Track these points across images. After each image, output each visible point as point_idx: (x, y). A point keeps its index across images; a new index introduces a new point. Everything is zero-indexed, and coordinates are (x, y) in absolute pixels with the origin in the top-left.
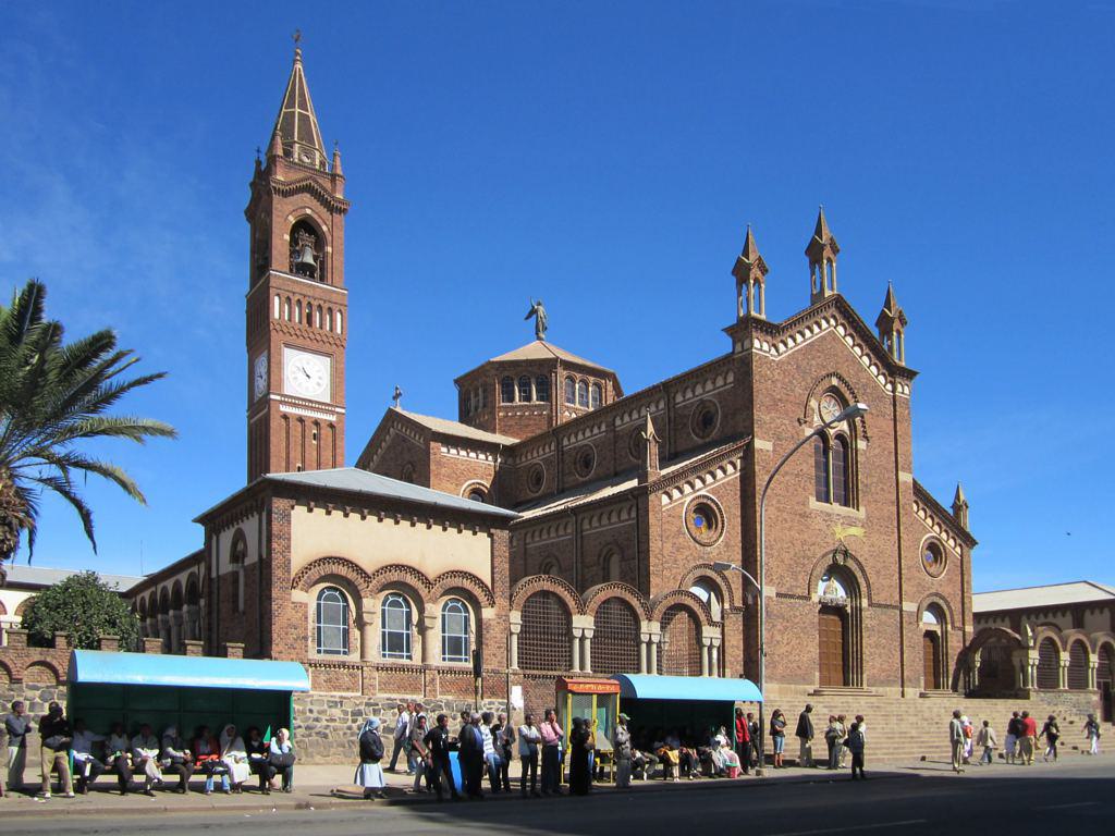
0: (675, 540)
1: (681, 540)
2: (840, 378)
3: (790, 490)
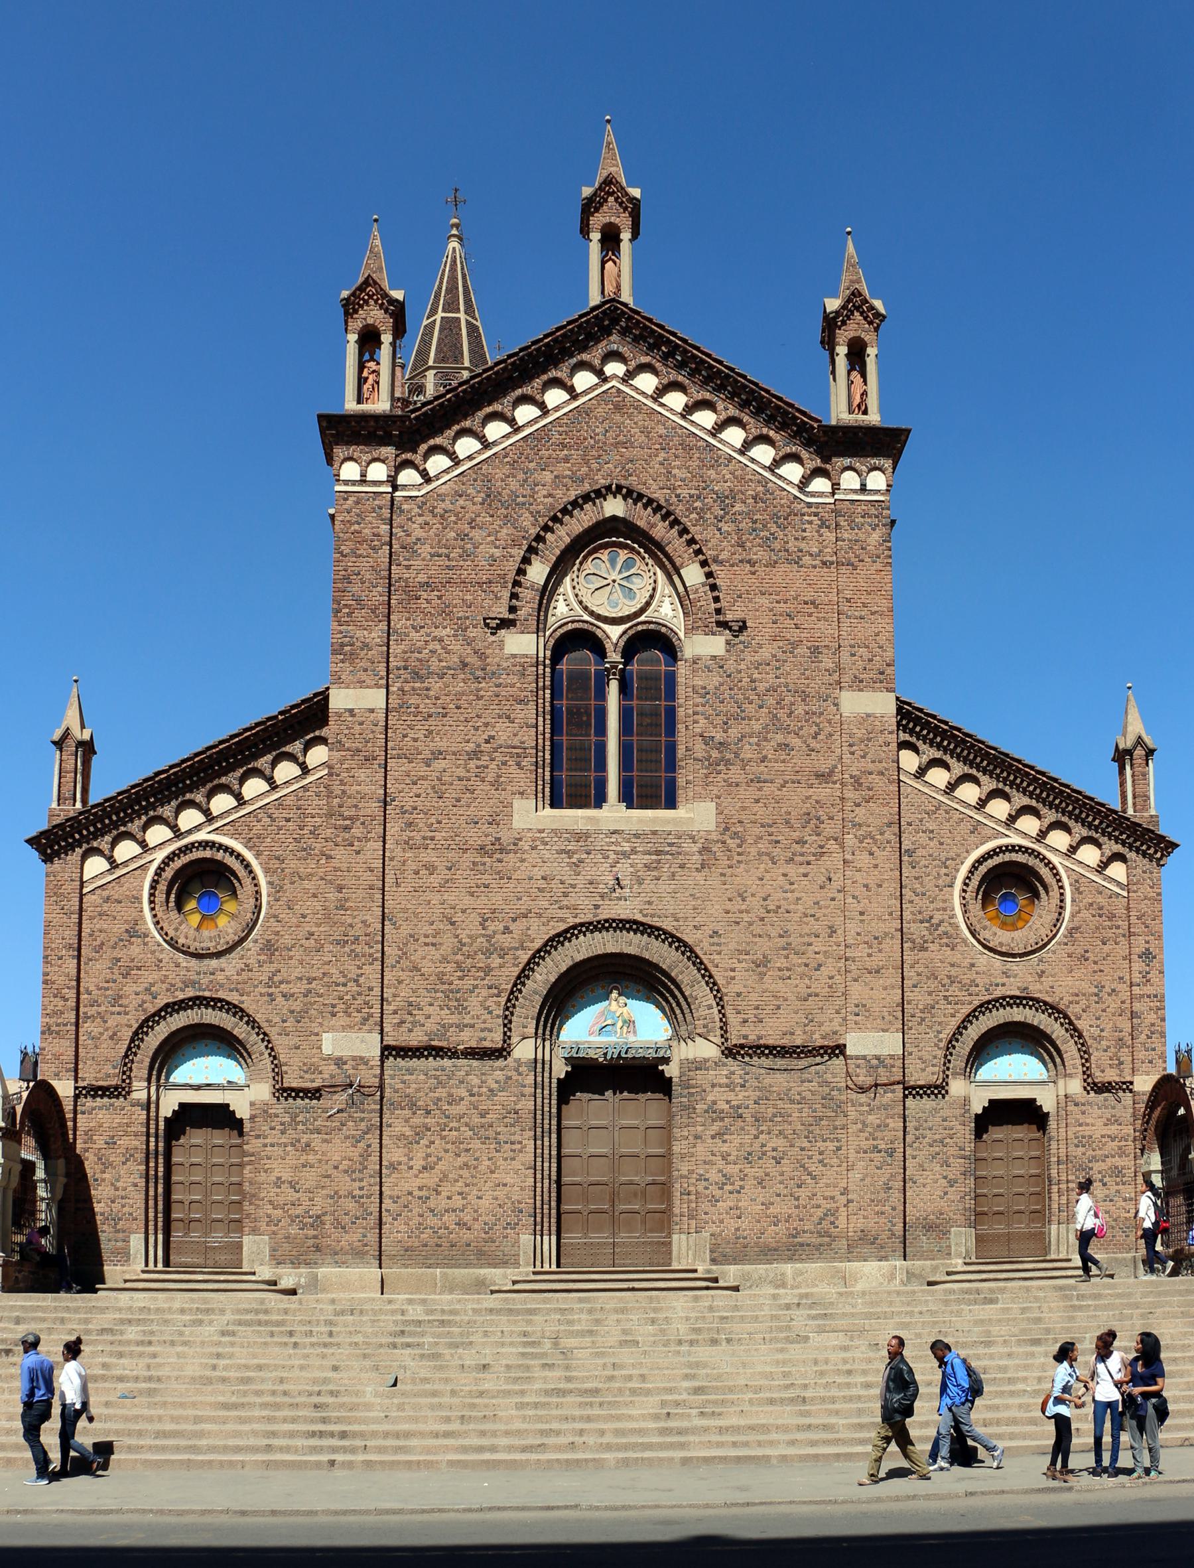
0: (117, 953)
1: (135, 950)
2: (630, 494)
3: (451, 794)
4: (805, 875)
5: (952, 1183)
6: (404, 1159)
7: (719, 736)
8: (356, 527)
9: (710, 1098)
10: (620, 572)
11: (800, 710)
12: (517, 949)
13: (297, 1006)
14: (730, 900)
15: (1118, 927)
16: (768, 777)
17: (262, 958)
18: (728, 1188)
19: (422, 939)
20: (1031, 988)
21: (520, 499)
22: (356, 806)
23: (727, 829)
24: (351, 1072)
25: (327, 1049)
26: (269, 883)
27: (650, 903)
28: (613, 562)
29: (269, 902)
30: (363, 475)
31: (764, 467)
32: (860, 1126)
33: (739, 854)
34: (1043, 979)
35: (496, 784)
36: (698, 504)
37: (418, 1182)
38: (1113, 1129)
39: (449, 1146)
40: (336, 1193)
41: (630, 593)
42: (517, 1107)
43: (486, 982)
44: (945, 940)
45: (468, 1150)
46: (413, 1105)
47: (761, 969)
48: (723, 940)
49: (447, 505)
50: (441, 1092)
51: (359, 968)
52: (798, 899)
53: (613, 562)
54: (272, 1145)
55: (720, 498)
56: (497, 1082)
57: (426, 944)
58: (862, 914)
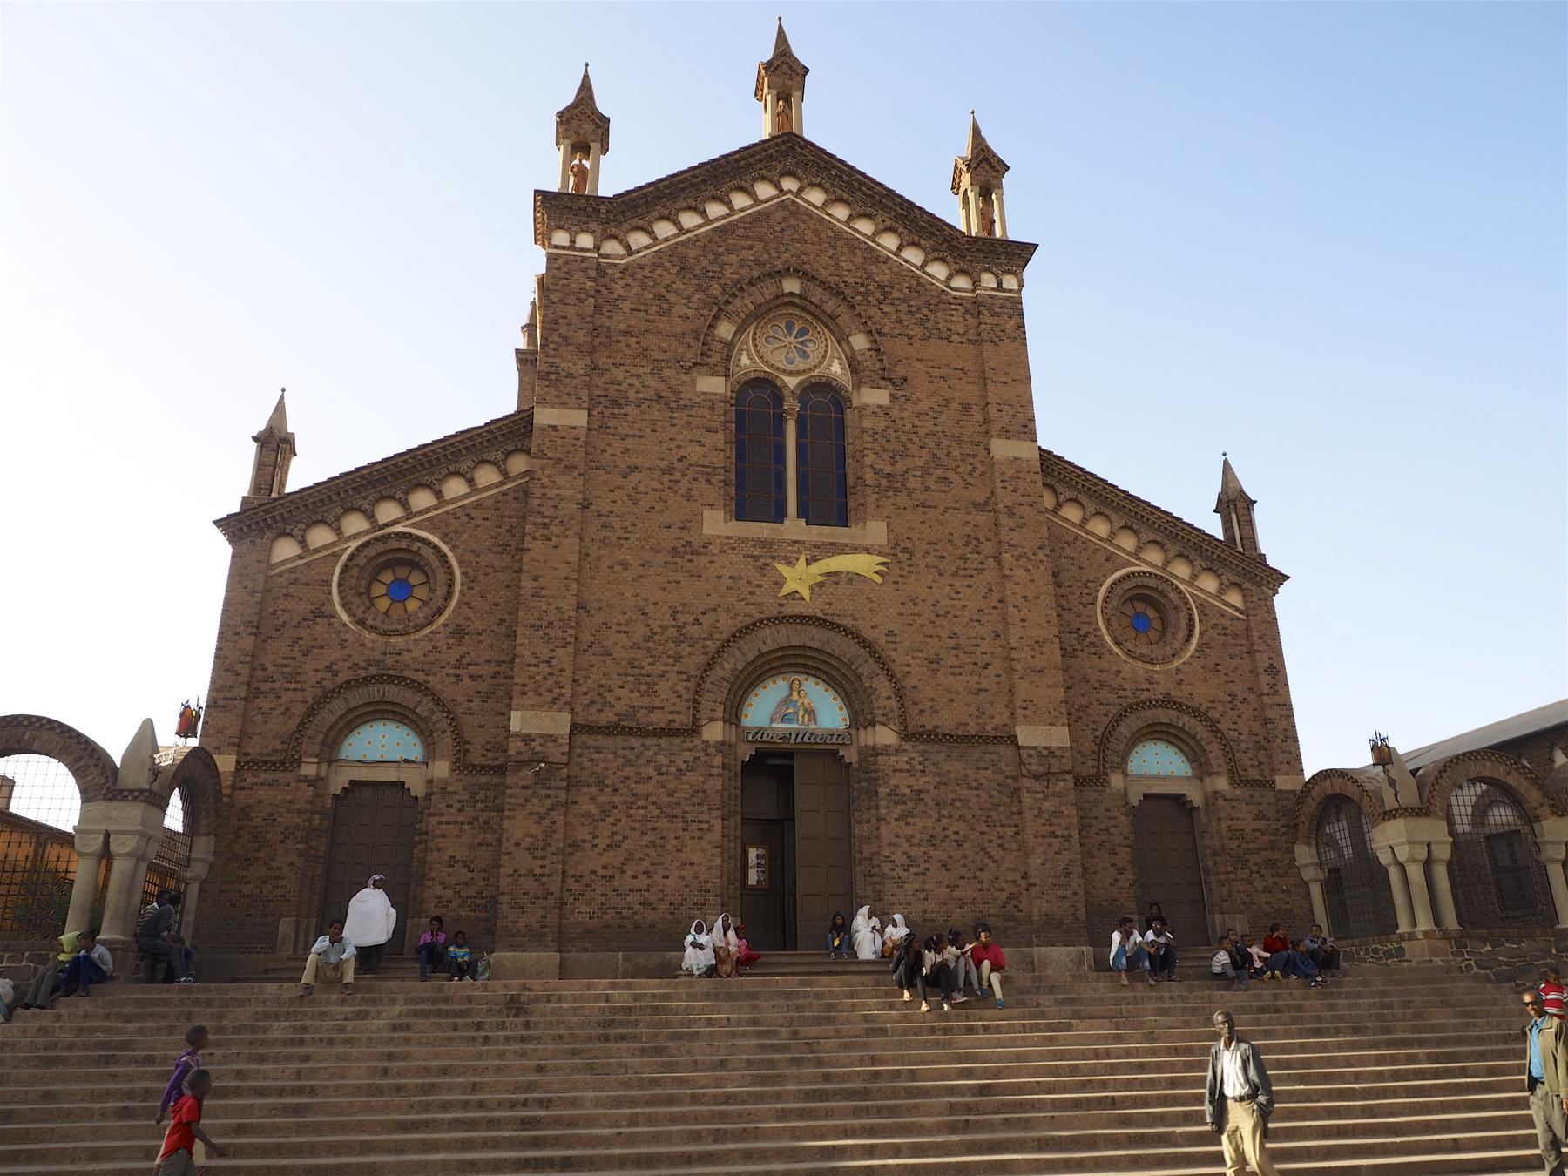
0: (300, 632)
1: (319, 629)
2: (807, 277)
4: (968, 586)
5: (1120, 871)
6: (589, 837)
7: (888, 469)
8: (565, 282)
9: (893, 782)
10: (796, 337)
11: (956, 452)
12: (706, 639)
13: (483, 687)
14: (902, 604)
15: (1242, 645)
16: (933, 504)
17: (451, 641)
18: (913, 870)
19: (615, 628)
20: (1172, 694)
21: (711, 274)
22: (555, 507)
23: (897, 544)
24: (538, 749)
25: (515, 726)
26: (463, 573)
27: (830, 604)
28: (789, 328)
29: (461, 591)
30: (573, 241)
31: (916, 267)
32: (1036, 812)
33: (909, 566)
34: (1182, 687)
35: (688, 497)
36: (862, 289)
37: (603, 860)
38: (1262, 824)
39: (636, 825)
40: (516, 871)
41: (804, 355)
42: (705, 787)
43: (676, 668)
44: (1092, 650)
45: (654, 829)
46: (600, 783)
47: (934, 666)
48: (898, 639)
49: (646, 272)
50: (629, 771)
51: (551, 650)
52: (964, 606)
53: (789, 328)
54: (448, 823)
55: (880, 286)
56: (685, 762)
57: (620, 632)
58: (1022, 620)
